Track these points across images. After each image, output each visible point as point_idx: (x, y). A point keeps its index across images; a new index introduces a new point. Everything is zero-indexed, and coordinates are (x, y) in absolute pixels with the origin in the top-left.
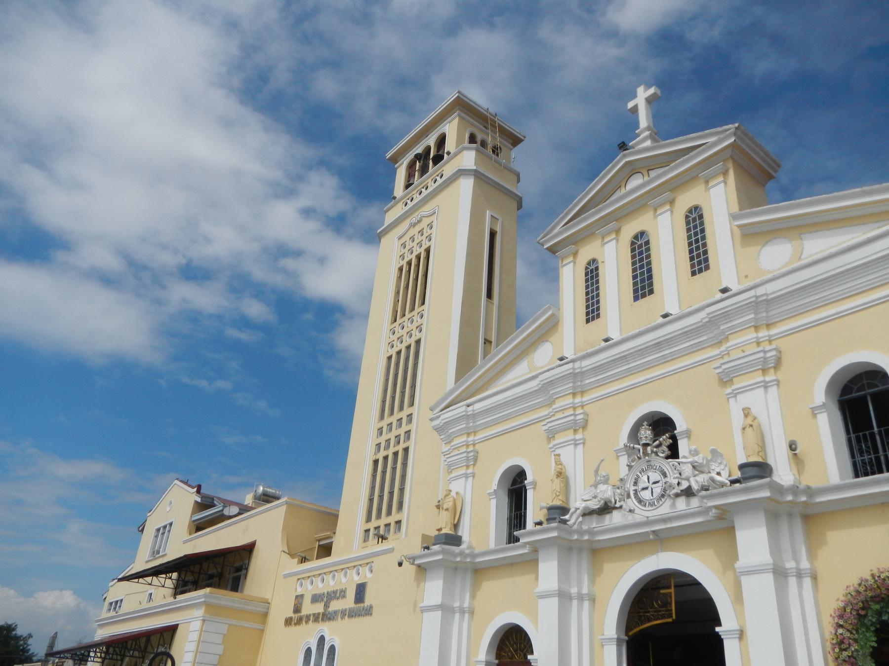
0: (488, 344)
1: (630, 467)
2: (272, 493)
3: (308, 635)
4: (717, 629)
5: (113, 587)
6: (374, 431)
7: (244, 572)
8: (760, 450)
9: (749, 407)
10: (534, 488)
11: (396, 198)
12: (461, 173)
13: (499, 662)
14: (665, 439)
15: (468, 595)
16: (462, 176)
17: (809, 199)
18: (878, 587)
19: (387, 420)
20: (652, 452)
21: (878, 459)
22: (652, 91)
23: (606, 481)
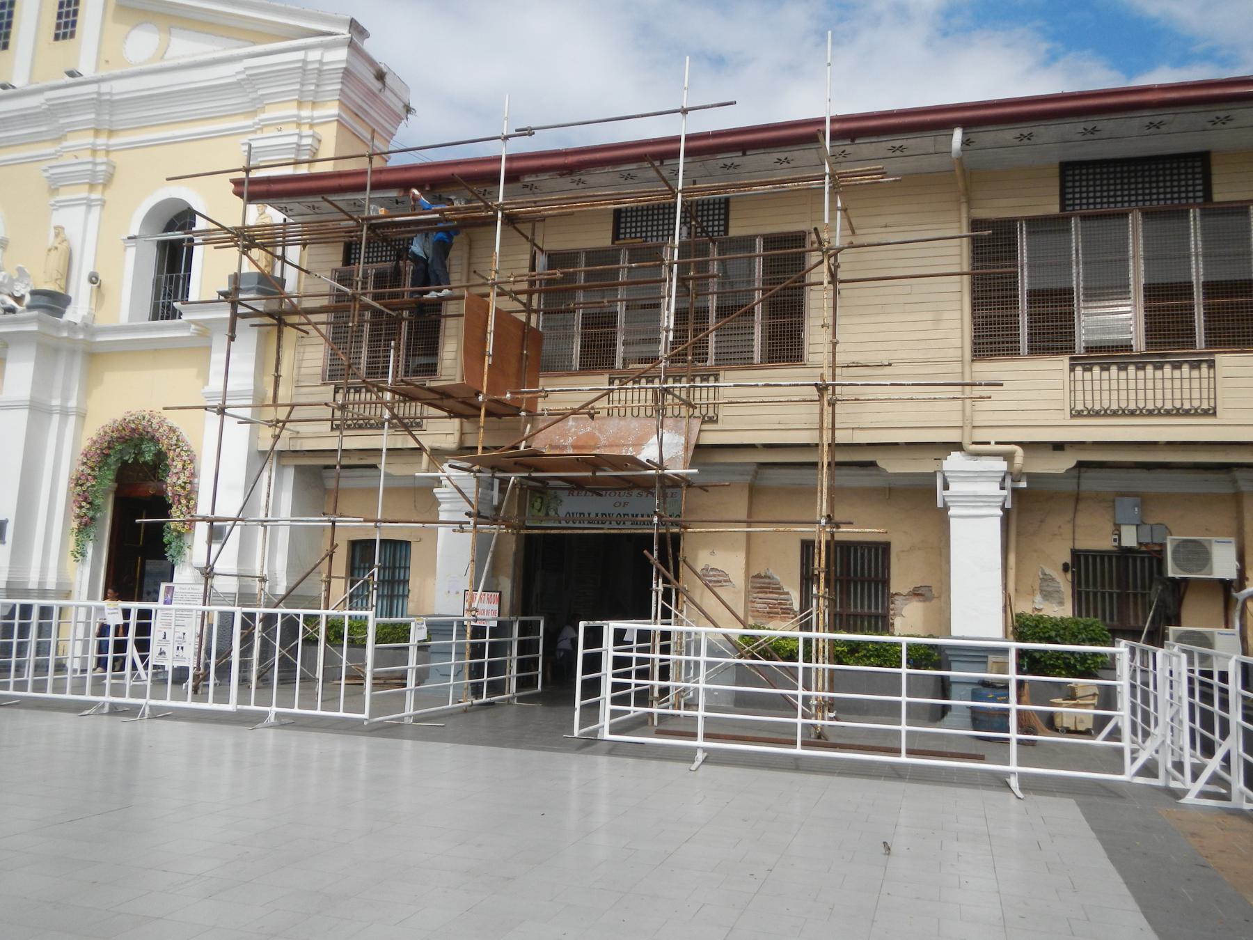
8: (59, 277)
9: (64, 226)
18: (124, 429)
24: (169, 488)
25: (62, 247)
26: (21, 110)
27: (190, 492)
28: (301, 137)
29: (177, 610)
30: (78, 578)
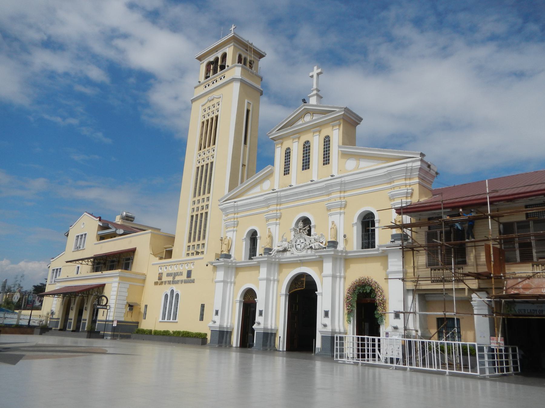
0: (244, 166)
1: (295, 236)
2: (131, 216)
3: (167, 289)
4: (316, 292)
5: (53, 262)
6: (191, 202)
7: (130, 261)
10: (260, 239)
11: (200, 82)
12: (233, 80)
13: (244, 301)
14: (307, 228)
15: (233, 277)
16: (234, 81)
17: (362, 147)
19: (197, 198)
20: (302, 232)
21: (369, 242)
22: (319, 71)
23: (286, 240)
24: (377, 301)
25: (335, 227)
26: (317, 187)
27: (383, 302)
28: (407, 190)
29: (390, 339)
30: (349, 328)
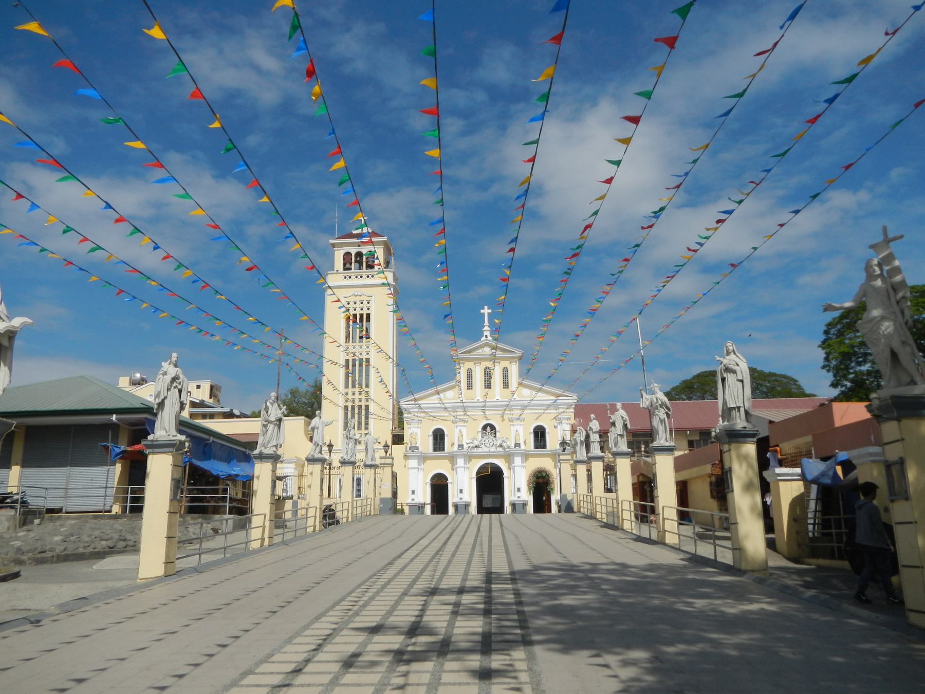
22: (490, 311)
